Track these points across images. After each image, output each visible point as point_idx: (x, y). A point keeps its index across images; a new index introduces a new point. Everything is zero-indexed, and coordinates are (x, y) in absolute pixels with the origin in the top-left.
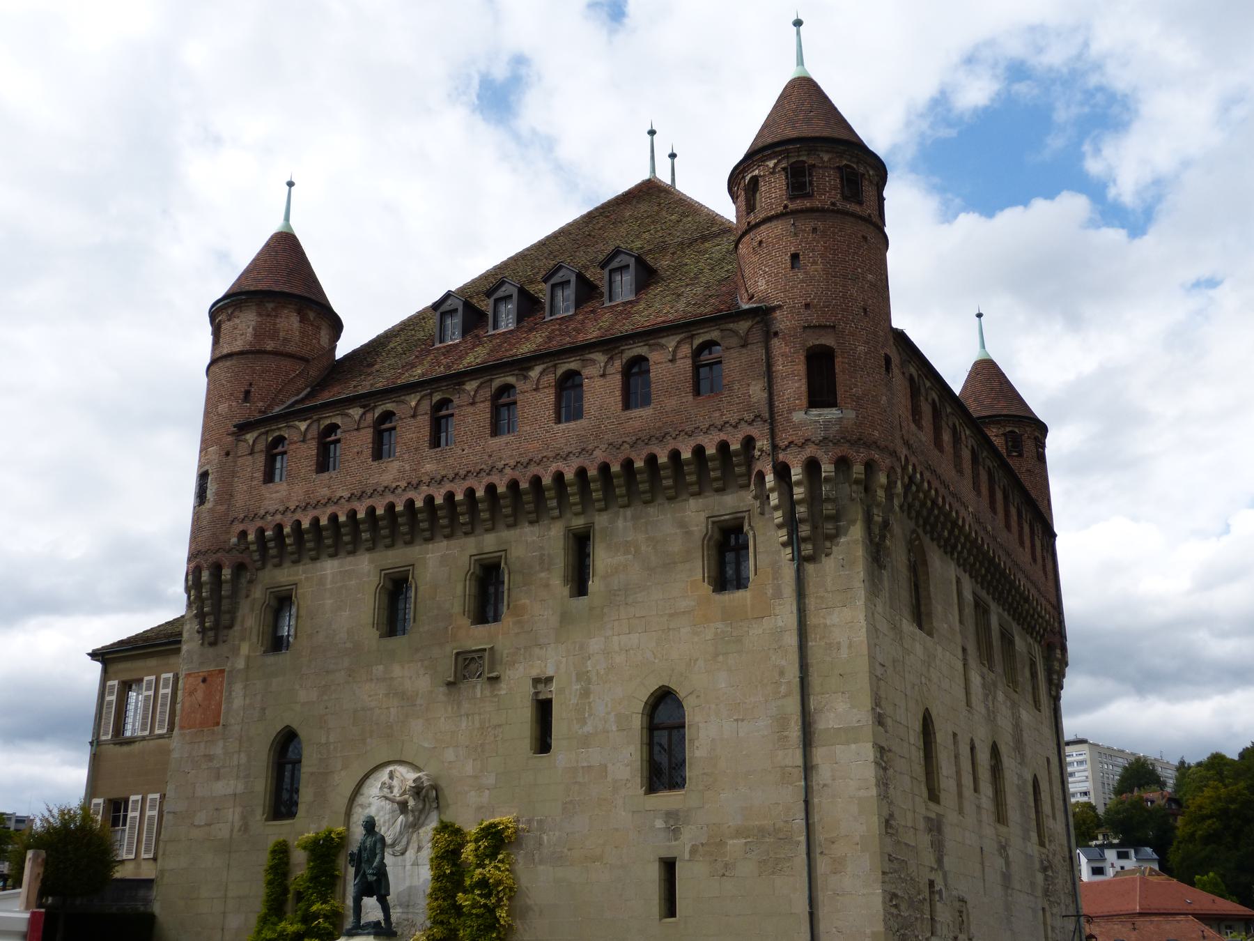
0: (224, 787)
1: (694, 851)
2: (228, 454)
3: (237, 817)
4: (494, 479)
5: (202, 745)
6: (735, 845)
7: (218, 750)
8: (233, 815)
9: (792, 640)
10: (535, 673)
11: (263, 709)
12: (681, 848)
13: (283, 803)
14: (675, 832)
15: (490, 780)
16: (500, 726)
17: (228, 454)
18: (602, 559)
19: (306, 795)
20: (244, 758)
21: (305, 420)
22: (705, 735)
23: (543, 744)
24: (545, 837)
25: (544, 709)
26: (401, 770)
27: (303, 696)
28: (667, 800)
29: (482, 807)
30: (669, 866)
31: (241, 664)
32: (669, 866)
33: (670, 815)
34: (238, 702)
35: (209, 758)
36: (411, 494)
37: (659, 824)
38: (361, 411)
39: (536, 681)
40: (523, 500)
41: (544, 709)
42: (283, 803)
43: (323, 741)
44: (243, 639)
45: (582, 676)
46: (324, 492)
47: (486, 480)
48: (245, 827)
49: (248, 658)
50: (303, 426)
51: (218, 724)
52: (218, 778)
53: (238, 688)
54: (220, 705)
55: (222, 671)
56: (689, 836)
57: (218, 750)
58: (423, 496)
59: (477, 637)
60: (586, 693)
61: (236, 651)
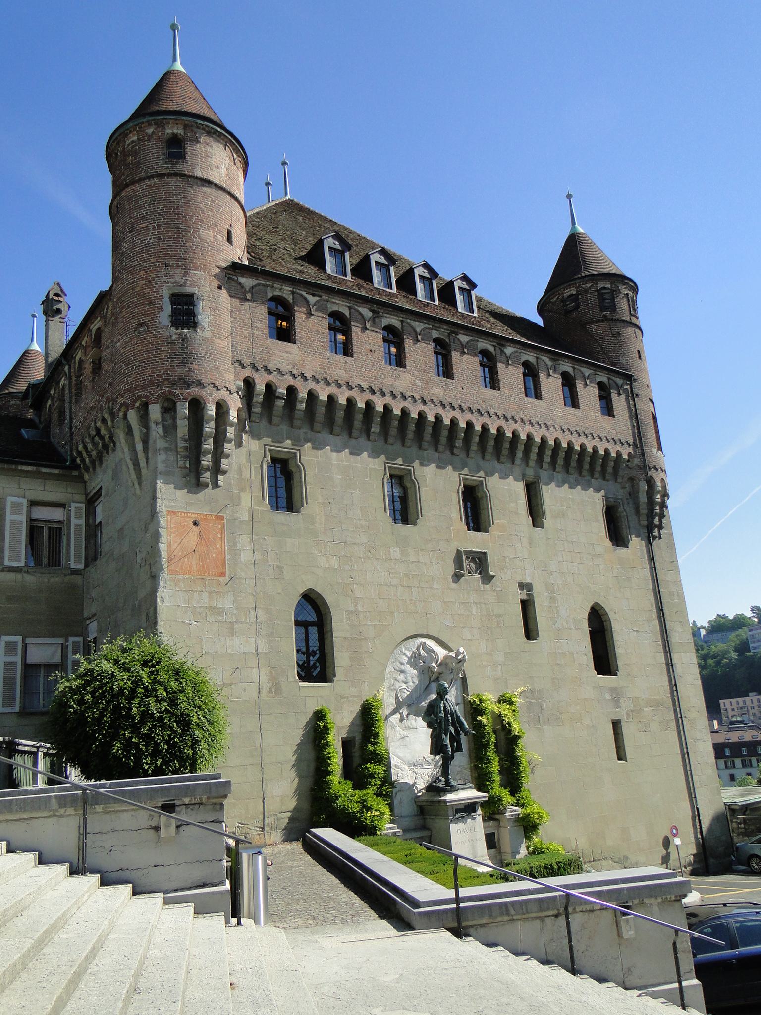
1: (628, 715)
3: (264, 679)
5: (205, 595)
7: (227, 602)
10: (519, 578)
11: (280, 568)
12: (621, 714)
13: (316, 665)
14: (616, 702)
15: (500, 658)
19: (341, 658)
21: (314, 295)
23: (530, 633)
24: (544, 704)
25: (527, 606)
27: (322, 561)
30: (616, 725)
31: (246, 517)
32: (616, 725)
34: (245, 556)
35: (217, 611)
37: (608, 697)
38: (370, 314)
41: (527, 606)
42: (316, 665)
43: (352, 608)
44: (242, 489)
48: (276, 689)
49: (252, 511)
51: (223, 574)
52: (232, 632)
53: (244, 540)
54: (223, 553)
55: (222, 518)
57: (227, 602)
58: (434, 413)
59: (475, 541)
60: (553, 599)
61: (236, 500)
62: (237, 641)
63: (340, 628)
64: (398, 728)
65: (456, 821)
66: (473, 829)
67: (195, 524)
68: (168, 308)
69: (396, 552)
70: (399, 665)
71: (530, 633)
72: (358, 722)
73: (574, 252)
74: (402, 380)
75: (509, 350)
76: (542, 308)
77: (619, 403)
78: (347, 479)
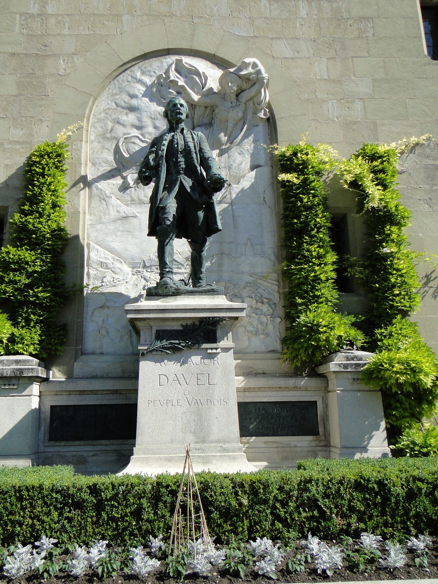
15: (363, 88)
16: (366, 19)
29: (355, 123)
64: (114, 201)
65: (157, 354)
66: (204, 380)
70: (127, 99)
72: (18, 183)
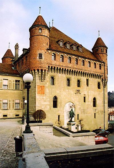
0: (46, 103)
2: (46, 52)
4: (82, 71)
6: (100, 112)
7: (45, 98)
8: (48, 107)
9: (103, 95)
14: (96, 111)
15: (80, 105)
17: (46, 52)
18: (90, 83)
20: (49, 99)
22: (98, 102)
25: (84, 98)
26: (71, 103)
27: (57, 92)
28: (95, 108)
32: (95, 114)
33: (95, 109)
35: (43, 99)
36: (75, 70)
39: (84, 95)
40: (84, 74)
45: (88, 95)
46: (62, 65)
47: (81, 71)
48: (50, 109)
50: (58, 53)
53: (47, 89)
56: (97, 111)
57: (45, 98)
60: (88, 97)
62: (46, 103)
63: (59, 101)
67: (41, 87)
68: (38, 55)
69: (67, 90)
71: (85, 101)
73: (99, 40)
74: (70, 65)
75: (86, 60)
76: (92, 49)
77: (102, 67)
78: (61, 78)
